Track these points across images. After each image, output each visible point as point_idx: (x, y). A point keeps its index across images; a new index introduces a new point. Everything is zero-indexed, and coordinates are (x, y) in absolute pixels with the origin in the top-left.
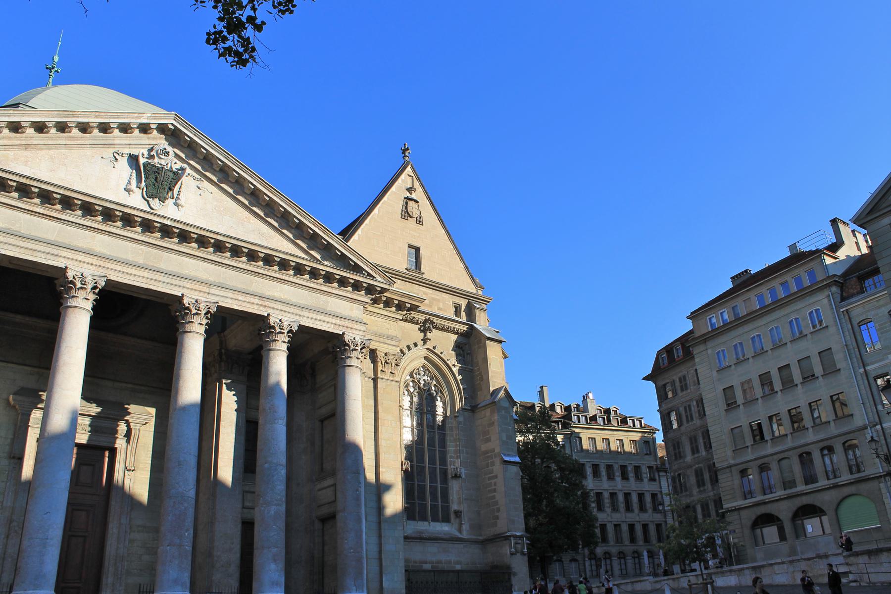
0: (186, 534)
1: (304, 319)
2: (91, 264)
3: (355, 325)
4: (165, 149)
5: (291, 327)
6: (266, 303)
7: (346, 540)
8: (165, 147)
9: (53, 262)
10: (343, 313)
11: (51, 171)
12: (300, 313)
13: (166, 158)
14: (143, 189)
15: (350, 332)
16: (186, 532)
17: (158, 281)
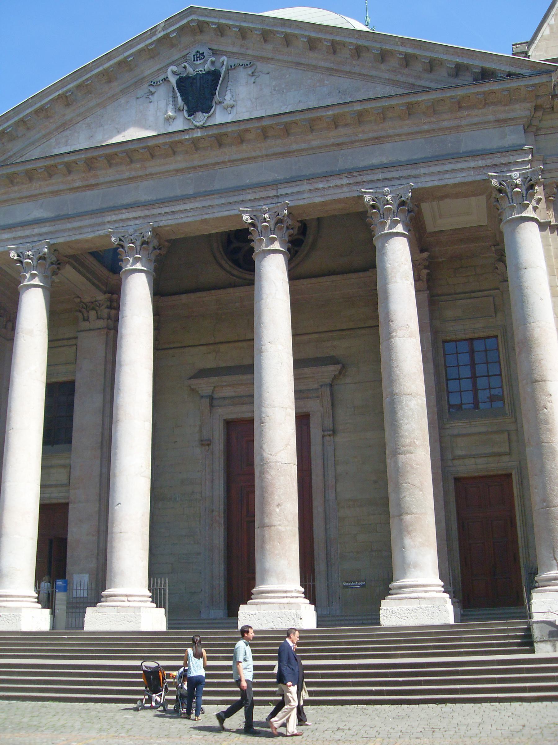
0: (278, 510)
1: (423, 179)
2: (137, 218)
3: (511, 157)
4: (198, 52)
5: (401, 197)
6: (359, 179)
7: (536, 488)
8: (197, 50)
9: (100, 232)
10: (488, 147)
11: (89, 138)
12: (414, 172)
13: (202, 61)
14: (183, 110)
15: (505, 170)
16: (279, 505)
17: (212, 206)
